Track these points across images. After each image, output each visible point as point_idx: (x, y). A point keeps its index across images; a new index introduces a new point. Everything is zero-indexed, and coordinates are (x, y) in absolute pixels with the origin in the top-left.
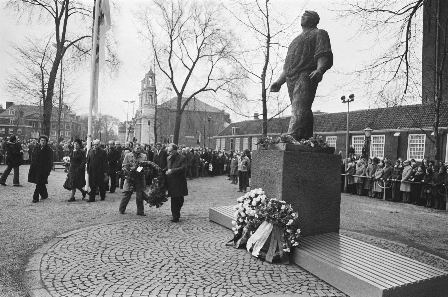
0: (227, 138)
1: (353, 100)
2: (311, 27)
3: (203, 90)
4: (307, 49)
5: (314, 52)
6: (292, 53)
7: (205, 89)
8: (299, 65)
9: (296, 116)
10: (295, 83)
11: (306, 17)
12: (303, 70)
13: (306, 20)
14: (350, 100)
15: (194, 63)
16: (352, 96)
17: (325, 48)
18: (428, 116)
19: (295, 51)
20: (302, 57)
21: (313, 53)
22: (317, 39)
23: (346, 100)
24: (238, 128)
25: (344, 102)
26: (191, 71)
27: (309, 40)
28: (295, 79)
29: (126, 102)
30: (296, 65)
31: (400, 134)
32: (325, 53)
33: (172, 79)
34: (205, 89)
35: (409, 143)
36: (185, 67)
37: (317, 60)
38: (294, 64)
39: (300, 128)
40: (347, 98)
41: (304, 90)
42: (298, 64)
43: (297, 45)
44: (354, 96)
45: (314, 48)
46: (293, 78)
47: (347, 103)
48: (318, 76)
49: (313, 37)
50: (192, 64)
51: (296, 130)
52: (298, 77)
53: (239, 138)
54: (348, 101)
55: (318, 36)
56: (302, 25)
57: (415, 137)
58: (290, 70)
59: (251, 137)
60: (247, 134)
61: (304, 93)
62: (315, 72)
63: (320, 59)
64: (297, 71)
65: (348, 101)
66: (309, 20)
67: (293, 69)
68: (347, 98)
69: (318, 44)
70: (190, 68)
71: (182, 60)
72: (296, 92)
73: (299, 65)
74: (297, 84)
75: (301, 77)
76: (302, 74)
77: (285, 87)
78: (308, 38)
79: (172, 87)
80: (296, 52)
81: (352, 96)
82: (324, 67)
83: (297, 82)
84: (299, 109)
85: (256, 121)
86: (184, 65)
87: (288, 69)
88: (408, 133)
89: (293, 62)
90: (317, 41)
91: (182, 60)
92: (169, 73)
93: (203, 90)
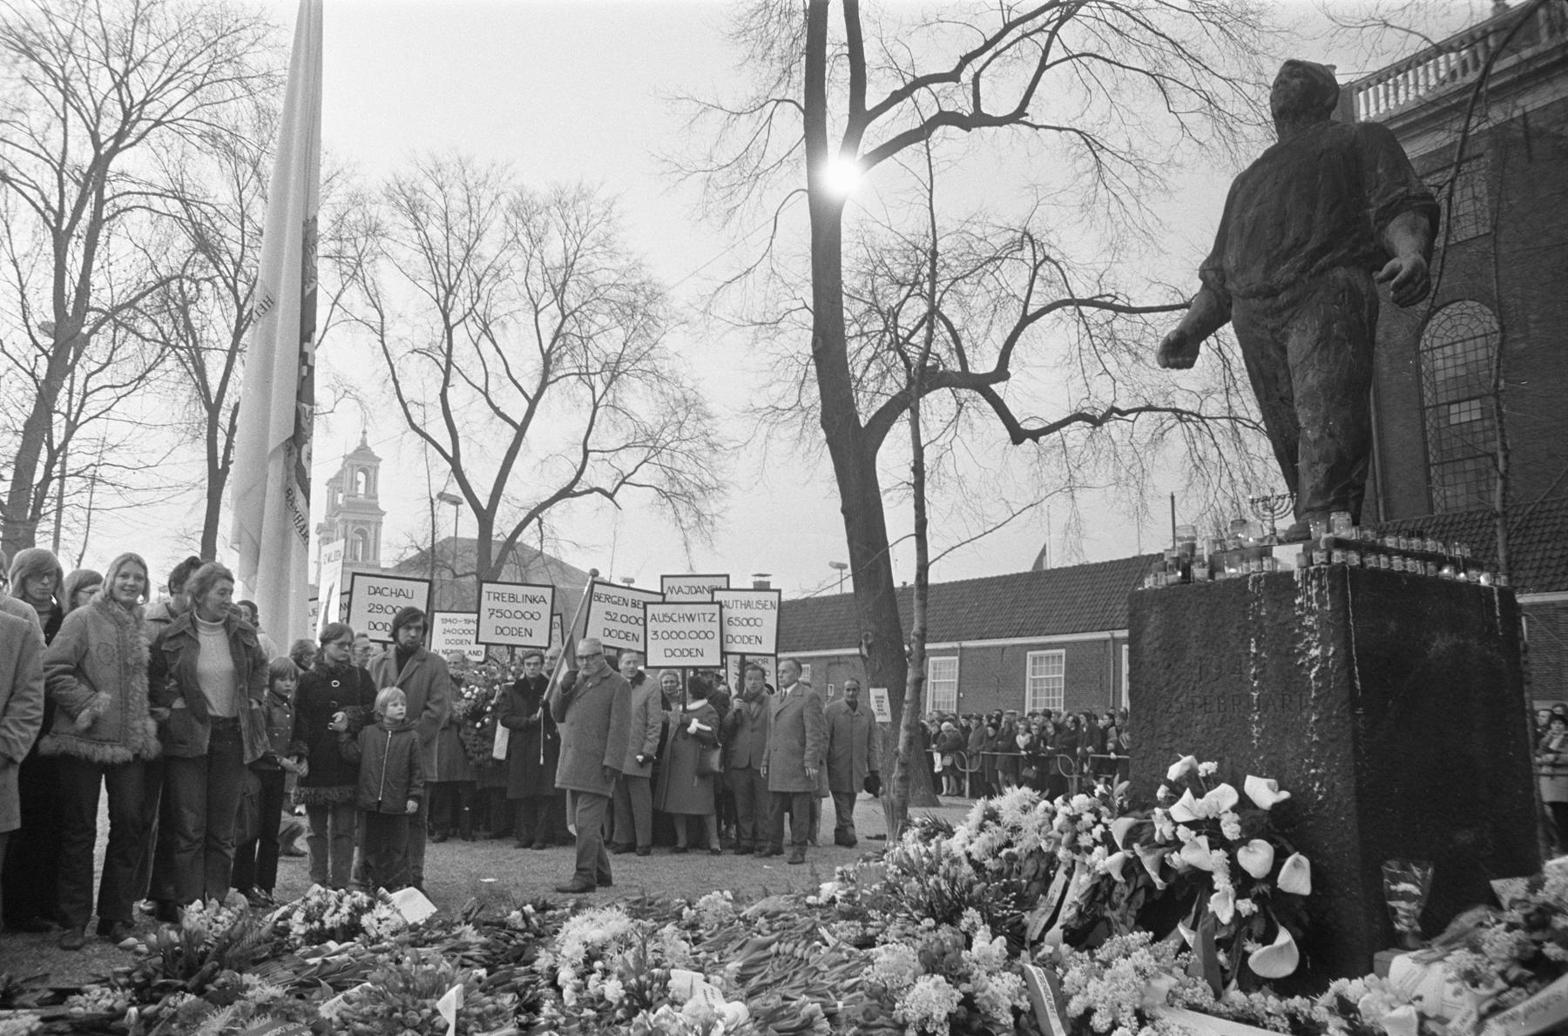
3: (566, 493)
9: (1331, 435)
15: (533, 403)
26: (521, 430)
28: (1293, 303)
30: (1298, 245)
33: (455, 461)
36: (498, 419)
42: (1306, 242)
46: (1283, 298)
50: (526, 405)
58: (1269, 268)
64: (1303, 270)
70: (519, 421)
71: (486, 394)
73: (1309, 247)
79: (455, 489)
86: (496, 410)
91: (486, 394)
92: (446, 442)
93: (566, 493)
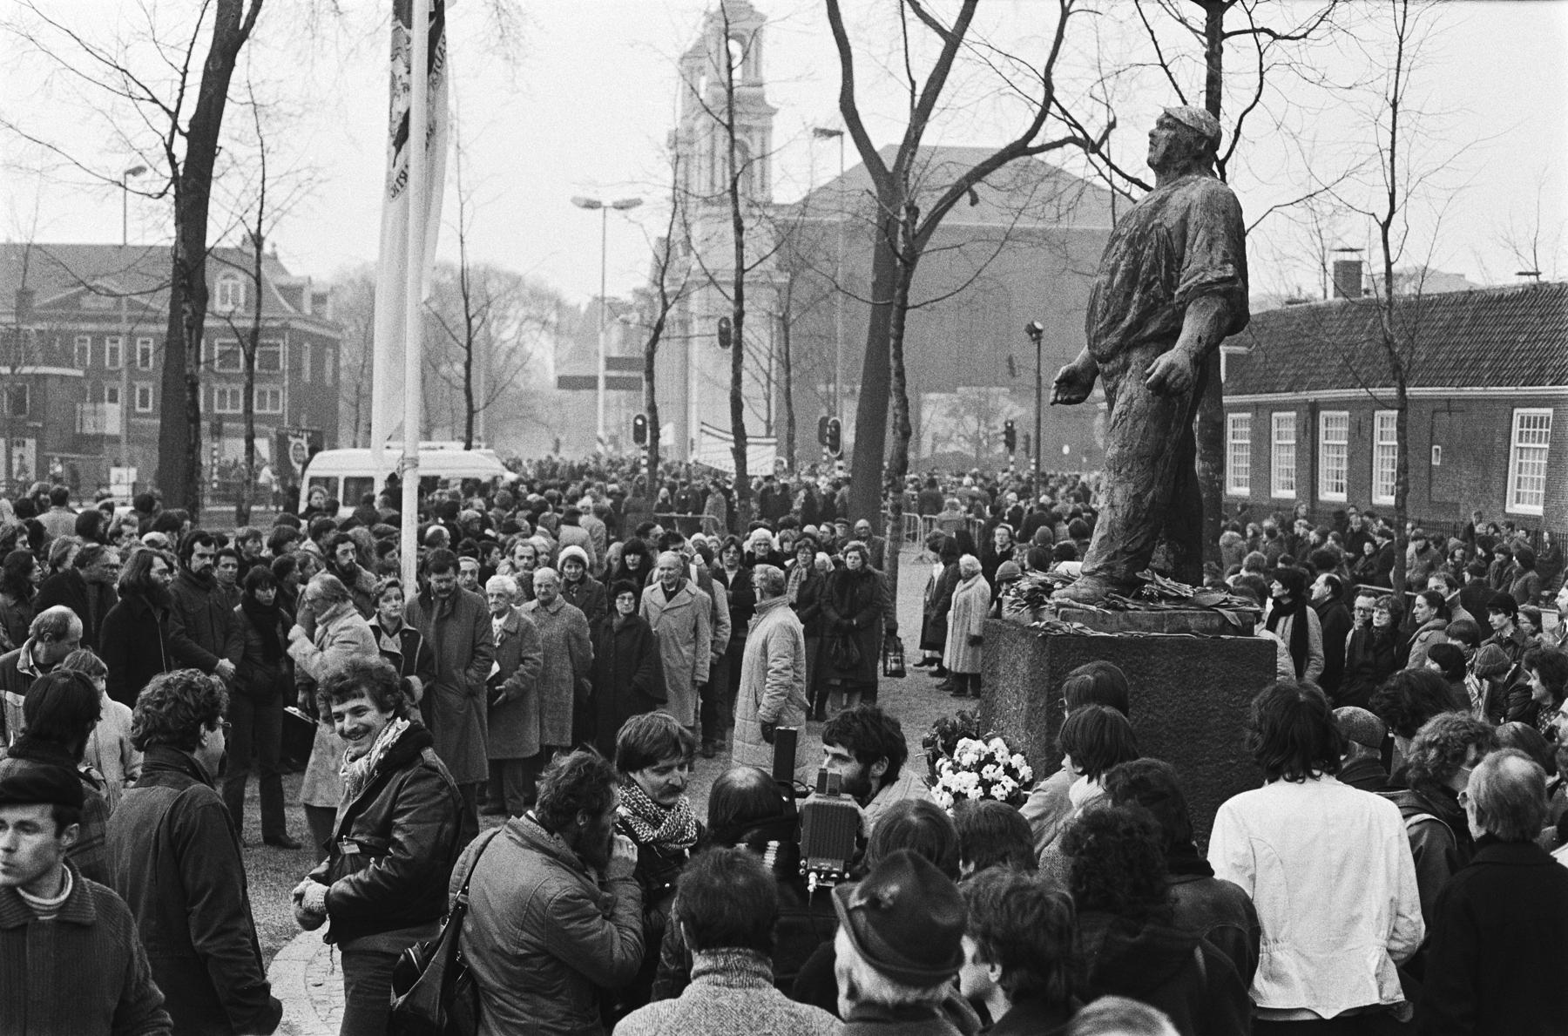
2: (1187, 170)
4: (1154, 268)
7: (1033, 144)
9: (1112, 506)
10: (1116, 386)
11: (1165, 133)
12: (1142, 343)
13: (1162, 148)
17: (1211, 262)
20: (1136, 297)
21: (1170, 284)
22: (1192, 226)
24: (1241, 350)
27: (1162, 231)
29: (591, 205)
32: (1209, 283)
34: (1033, 144)
37: (1184, 309)
39: (1124, 550)
41: (1140, 415)
45: (1181, 260)
48: (1173, 375)
49: (1178, 218)
52: (1126, 367)
53: (1248, 415)
55: (1195, 216)
56: (1150, 164)
59: (1314, 408)
60: (1289, 390)
61: (1141, 425)
63: (1191, 307)
66: (1173, 144)
67: (1107, 335)
75: (1133, 367)
76: (1136, 356)
78: (1160, 225)
80: (1118, 278)
82: (1200, 339)
85: (1343, 309)
89: (1107, 310)
90: (1191, 233)
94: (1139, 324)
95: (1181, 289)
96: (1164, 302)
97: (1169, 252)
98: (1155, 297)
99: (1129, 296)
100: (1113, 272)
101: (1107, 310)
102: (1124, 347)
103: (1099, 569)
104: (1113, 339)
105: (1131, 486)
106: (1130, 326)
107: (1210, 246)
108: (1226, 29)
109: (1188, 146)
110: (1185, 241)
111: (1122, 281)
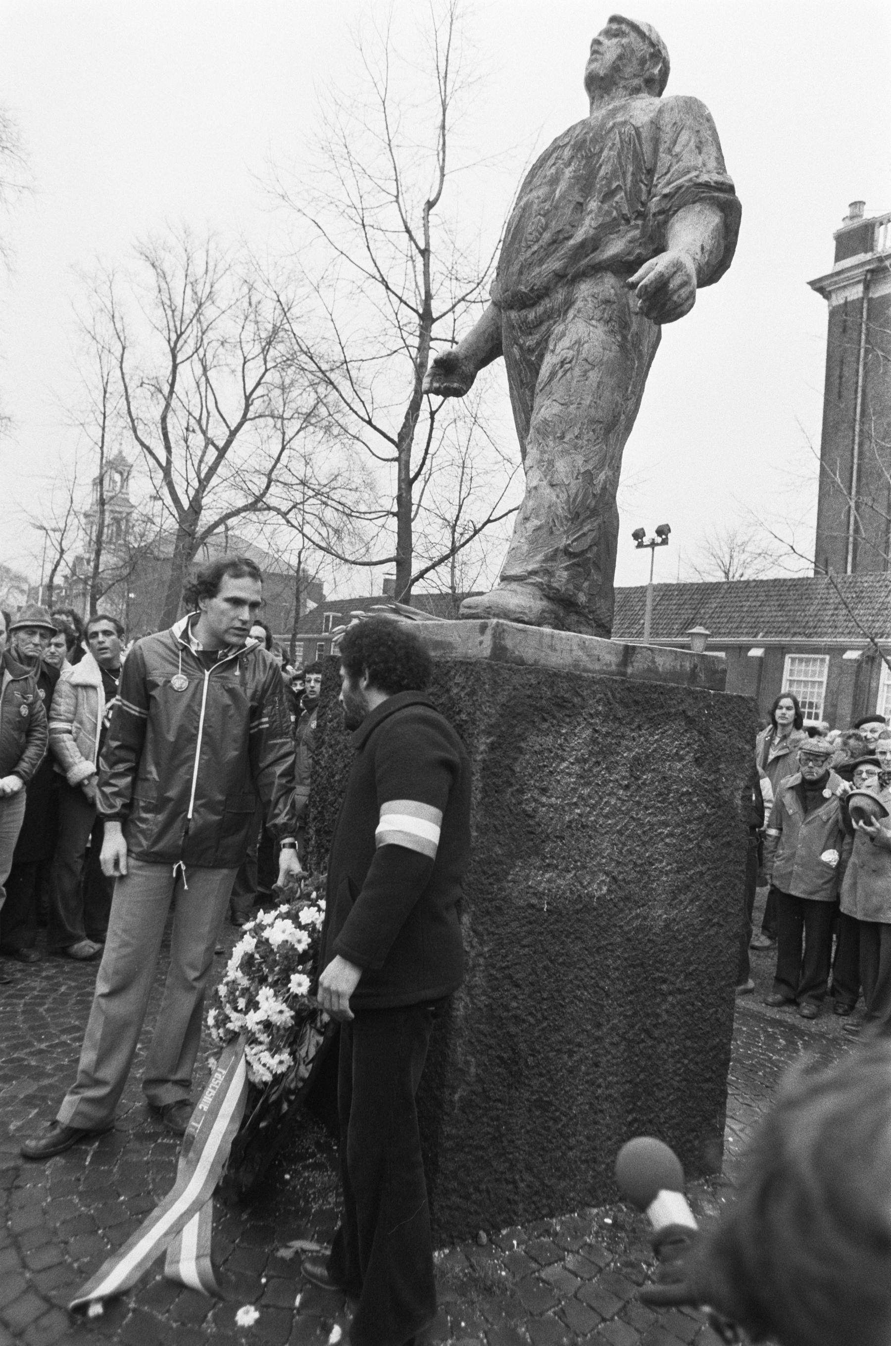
0: (309, 640)
1: (665, 542)
4: (618, 172)
5: (650, 186)
6: (541, 192)
8: (572, 242)
10: (545, 340)
12: (596, 269)
13: (610, 55)
14: (659, 540)
16: (663, 531)
18: (836, 609)
19: (554, 181)
23: (646, 541)
25: (640, 545)
31: (766, 653)
32: (706, 185)
35: (786, 675)
37: (666, 222)
38: (547, 236)
39: (566, 552)
40: (650, 535)
43: (567, 153)
44: (669, 531)
45: (651, 172)
47: (649, 549)
51: (544, 561)
52: (569, 303)
54: (653, 544)
57: (801, 660)
61: (594, 376)
62: (659, 264)
64: (559, 276)
65: (653, 544)
67: (541, 262)
68: (650, 535)
69: (669, 151)
72: (553, 375)
74: (563, 335)
75: (579, 304)
76: (585, 289)
77: (494, 377)
78: (625, 123)
81: (663, 531)
83: (558, 329)
84: (565, 453)
87: (515, 268)
88: (783, 650)
94: (593, 244)
95: (666, 191)
96: (628, 221)
97: (637, 157)
98: (618, 208)
99: (580, 206)
100: (554, 181)
101: (545, 228)
102: (569, 278)
103: (534, 573)
104: (554, 264)
105: (580, 460)
106: (583, 244)
107: (699, 149)
108: (433, 335)
109: (642, 62)
110: (656, 151)
111: (571, 187)
